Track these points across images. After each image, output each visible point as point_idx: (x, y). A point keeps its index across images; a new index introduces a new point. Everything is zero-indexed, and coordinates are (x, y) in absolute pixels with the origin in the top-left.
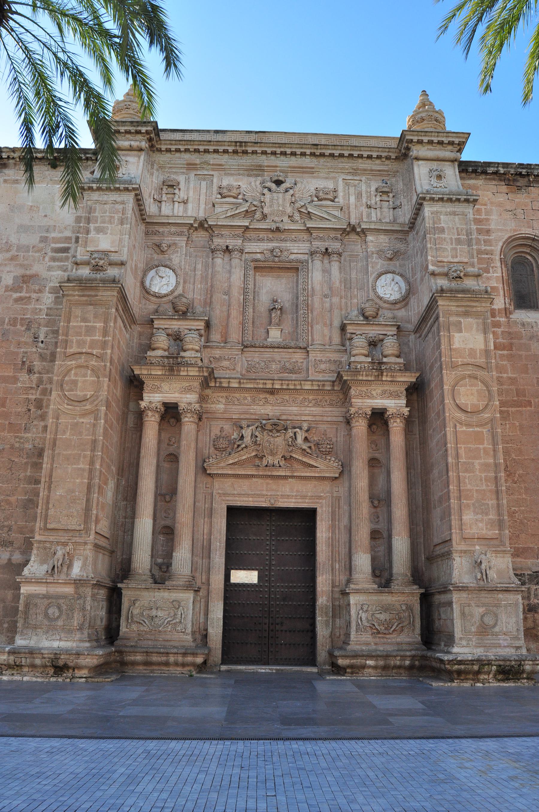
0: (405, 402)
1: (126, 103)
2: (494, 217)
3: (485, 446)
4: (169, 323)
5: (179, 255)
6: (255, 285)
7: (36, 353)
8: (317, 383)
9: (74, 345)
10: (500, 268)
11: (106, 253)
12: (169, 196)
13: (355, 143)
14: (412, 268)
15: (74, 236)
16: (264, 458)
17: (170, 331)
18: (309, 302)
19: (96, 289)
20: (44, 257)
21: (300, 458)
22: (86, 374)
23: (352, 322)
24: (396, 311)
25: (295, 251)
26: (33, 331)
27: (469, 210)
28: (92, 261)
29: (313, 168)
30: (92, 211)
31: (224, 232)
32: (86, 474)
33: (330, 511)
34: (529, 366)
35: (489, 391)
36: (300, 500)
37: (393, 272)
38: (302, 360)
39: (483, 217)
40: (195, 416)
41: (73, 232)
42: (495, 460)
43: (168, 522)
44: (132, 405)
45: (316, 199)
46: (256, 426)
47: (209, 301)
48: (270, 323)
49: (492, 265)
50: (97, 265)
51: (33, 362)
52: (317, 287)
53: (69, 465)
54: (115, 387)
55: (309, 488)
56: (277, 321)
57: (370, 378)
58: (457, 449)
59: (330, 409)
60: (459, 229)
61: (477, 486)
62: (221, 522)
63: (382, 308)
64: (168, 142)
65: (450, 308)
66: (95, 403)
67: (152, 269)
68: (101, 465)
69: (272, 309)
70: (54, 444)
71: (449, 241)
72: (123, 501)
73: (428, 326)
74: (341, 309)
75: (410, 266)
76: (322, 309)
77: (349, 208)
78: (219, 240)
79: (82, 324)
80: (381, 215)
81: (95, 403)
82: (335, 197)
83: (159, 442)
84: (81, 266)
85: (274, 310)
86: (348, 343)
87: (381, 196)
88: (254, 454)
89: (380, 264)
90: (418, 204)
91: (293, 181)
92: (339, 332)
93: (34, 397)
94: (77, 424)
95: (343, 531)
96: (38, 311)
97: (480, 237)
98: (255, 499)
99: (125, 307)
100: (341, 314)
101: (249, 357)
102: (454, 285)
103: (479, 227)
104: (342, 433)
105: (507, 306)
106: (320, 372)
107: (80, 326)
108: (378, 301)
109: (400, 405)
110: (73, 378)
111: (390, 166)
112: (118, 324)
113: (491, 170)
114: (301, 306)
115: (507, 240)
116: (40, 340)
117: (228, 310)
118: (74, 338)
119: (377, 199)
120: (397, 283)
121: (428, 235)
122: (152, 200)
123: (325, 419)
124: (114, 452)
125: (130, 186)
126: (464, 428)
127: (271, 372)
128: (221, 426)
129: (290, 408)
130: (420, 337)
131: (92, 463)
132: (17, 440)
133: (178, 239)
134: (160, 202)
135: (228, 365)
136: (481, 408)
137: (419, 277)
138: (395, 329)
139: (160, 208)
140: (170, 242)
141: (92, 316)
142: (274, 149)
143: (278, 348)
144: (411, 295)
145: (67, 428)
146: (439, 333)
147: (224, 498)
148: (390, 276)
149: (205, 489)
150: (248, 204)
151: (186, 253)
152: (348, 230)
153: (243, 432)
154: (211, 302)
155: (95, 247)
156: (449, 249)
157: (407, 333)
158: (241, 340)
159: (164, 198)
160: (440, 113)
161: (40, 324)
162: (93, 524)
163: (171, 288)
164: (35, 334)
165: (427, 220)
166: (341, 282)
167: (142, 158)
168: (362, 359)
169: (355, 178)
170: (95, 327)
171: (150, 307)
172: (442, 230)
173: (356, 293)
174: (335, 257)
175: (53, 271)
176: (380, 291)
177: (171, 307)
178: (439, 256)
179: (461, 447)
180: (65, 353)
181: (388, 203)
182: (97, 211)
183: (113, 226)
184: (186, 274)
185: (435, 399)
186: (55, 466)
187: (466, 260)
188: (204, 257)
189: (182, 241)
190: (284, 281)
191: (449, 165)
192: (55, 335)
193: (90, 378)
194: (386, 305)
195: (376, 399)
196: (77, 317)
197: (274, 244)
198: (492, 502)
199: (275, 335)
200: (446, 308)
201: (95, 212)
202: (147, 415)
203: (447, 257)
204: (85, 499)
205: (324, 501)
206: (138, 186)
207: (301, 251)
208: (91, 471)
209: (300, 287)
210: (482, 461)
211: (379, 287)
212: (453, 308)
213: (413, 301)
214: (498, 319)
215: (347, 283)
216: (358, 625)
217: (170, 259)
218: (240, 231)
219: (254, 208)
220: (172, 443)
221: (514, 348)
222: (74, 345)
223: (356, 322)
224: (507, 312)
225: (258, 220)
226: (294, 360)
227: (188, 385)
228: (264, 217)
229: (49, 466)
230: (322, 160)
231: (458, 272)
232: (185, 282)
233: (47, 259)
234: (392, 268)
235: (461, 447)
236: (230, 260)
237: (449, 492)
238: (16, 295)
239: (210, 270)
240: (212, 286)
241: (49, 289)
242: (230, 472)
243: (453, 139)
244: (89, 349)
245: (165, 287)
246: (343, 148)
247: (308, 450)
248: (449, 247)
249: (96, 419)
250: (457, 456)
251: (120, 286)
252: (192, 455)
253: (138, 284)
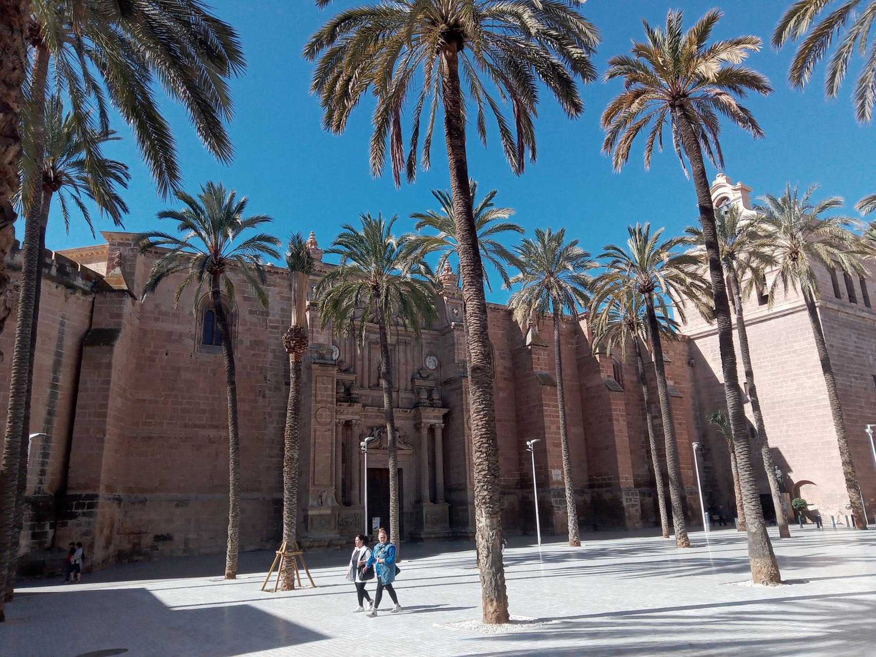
32: (330, 458)
131: (332, 453)
216: (426, 520)
238: (252, 352)
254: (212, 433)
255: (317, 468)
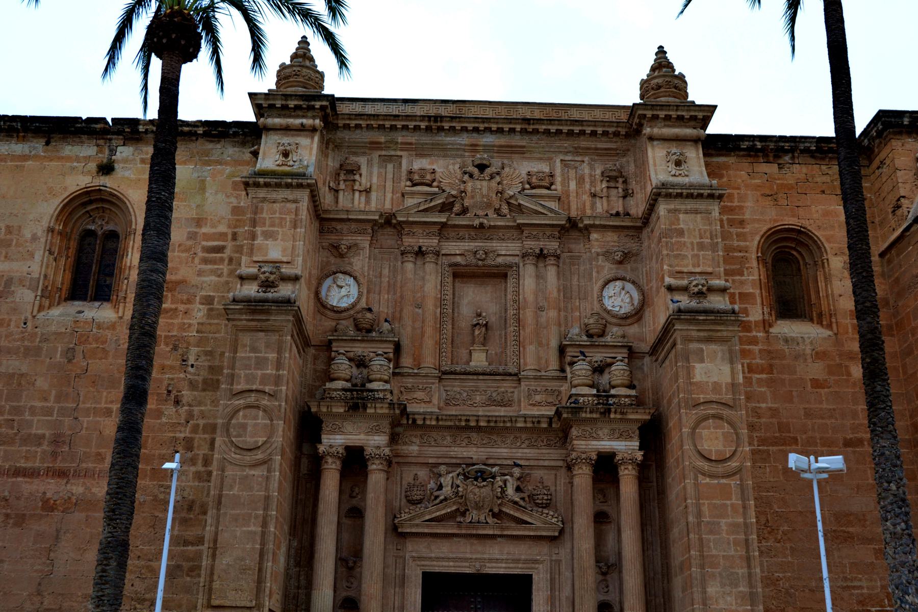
0: (638, 444)
1: (295, 69)
2: (749, 203)
3: (734, 501)
4: (351, 345)
5: (361, 258)
6: (454, 294)
7: (184, 379)
8: (531, 419)
9: (242, 380)
10: (757, 270)
11: (276, 264)
12: (347, 183)
13: (575, 115)
14: (646, 273)
15: (230, 231)
16: (468, 513)
17: (351, 355)
18: (521, 316)
19: (267, 312)
20: (193, 258)
21: (512, 513)
22: (257, 416)
23: (573, 343)
24: (627, 328)
25: (503, 253)
26: (180, 351)
27: (715, 208)
28: (261, 276)
29: (524, 147)
30: (259, 211)
31: (417, 230)
33: (549, 578)
34: (794, 394)
35: (737, 434)
36: (511, 565)
37: (623, 279)
38: (512, 390)
39: (736, 204)
40: (385, 463)
41: (229, 227)
42: (745, 519)
43: (351, 593)
44: (306, 448)
45: (527, 186)
46: (457, 472)
47: (399, 316)
48: (473, 343)
49: (747, 265)
50: (267, 281)
51: (180, 392)
52: (530, 298)
53: (237, 527)
54: (289, 430)
55: (522, 551)
56: (482, 339)
57: (594, 416)
58: (698, 506)
59: (548, 451)
60: (702, 231)
61: (725, 551)
62: (416, 593)
63: (610, 324)
64: (346, 117)
65: (689, 333)
66: (269, 451)
67: (328, 277)
68: (275, 528)
69: (475, 325)
70: (220, 503)
71: (689, 246)
72: (295, 567)
73: (665, 350)
74: (560, 325)
75: (644, 270)
76: (537, 325)
77: (568, 196)
78: (410, 240)
79: (251, 355)
80: (608, 205)
81: (269, 451)
82: (552, 184)
83: (341, 492)
84: (246, 281)
85: (478, 326)
86: (568, 369)
87: (608, 181)
88: (454, 508)
89: (608, 269)
90: (652, 199)
91: (500, 164)
92: (558, 354)
93: (182, 435)
94: (247, 477)
95: (564, 603)
96: (186, 326)
97: (731, 230)
98: (457, 564)
99: (299, 330)
100: (560, 331)
101: (447, 386)
102: (694, 304)
103: (730, 217)
104: (563, 481)
105: (767, 317)
106: (534, 405)
107: (249, 357)
108: (605, 315)
109: (632, 447)
110: (241, 421)
111: (619, 144)
112: (293, 354)
113: (744, 145)
114: (511, 321)
115: (765, 233)
116: (190, 363)
117: (422, 328)
118: (242, 372)
119: (604, 186)
120: (628, 292)
121: (664, 239)
122: (327, 188)
123: (541, 463)
124: (286, 507)
125: (305, 182)
126: (708, 480)
127: (475, 405)
128: (415, 472)
129: (499, 450)
130: (656, 360)
131: (265, 524)
132: (162, 489)
133: (359, 238)
134: (337, 191)
135: (423, 397)
136: (728, 456)
137: (655, 286)
138: (625, 350)
139: (337, 198)
140: (351, 241)
141: (263, 344)
142: (476, 125)
143: (483, 374)
144: (645, 307)
145: (235, 482)
146: (676, 362)
147: (419, 563)
148: (619, 284)
149: (395, 551)
150: (445, 195)
151: (369, 256)
152: (567, 225)
153: (442, 480)
154: (401, 318)
155: (263, 256)
156: (690, 257)
157: (641, 355)
158: (437, 364)
159: (342, 186)
160: (681, 77)
161: (189, 344)
162: (267, 599)
163: (353, 301)
164: (183, 356)
165: (662, 220)
166: (559, 291)
167: (316, 139)
168: (586, 390)
169: (576, 159)
170: (267, 359)
171: (326, 324)
172: (681, 233)
173: (578, 304)
174: (552, 261)
175: (205, 276)
176: (608, 303)
177: (353, 324)
178: (677, 265)
179: (704, 504)
180: (231, 390)
181: (616, 190)
182: (265, 211)
183: (284, 229)
184: (369, 281)
185: (674, 441)
186: (220, 528)
187: (710, 270)
188: (392, 259)
189: (364, 241)
190: (489, 288)
191: (691, 145)
192: (209, 358)
193: (262, 420)
194: (614, 320)
195: (603, 440)
196: (245, 346)
197: (476, 244)
198: (742, 571)
199: (479, 360)
200: (685, 333)
201: (262, 213)
202: (327, 462)
203: (687, 266)
204: (257, 569)
205: (541, 566)
206: (314, 181)
207: (511, 253)
208: (263, 534)
209: (509, 297)
210: (730, 520)
211: (607, 297)
212: (694, 334)
213: (648, 314)
214: (754, 333)
215: (566, 292)
217: (351, 264)
218: (435, 229)
219: (452, 200)
220: (354, 494)
221: (775, 371)
222: (242, 380)
223: (578, 343)
224: (766, 325)
225: (456, 215)
226: (503, 389)
227: (375, 424)
228: (464, 211)
229: (213, 528)
230: (535, 138)
231: (700, 287)
232: (368, 292)
233: (197, 261)
234: (621, 273)
235: (704, 504)
236: (424, 264)
237: (690, 558)
239: (399, 277)
240: (402, 297)
241: (200, 299)
242: (426, 531)
243: (697, 114)
244: (260, 385)
245: (345, 299)
246: (560, 123)
247: (522, 503)
248: (689, 254)
249: (269, 471)
250: (699, 514)
251: (296, 308)
252: (381, 511)
253: (312, 296)
254: (52, 488)
255: (224, 561)
